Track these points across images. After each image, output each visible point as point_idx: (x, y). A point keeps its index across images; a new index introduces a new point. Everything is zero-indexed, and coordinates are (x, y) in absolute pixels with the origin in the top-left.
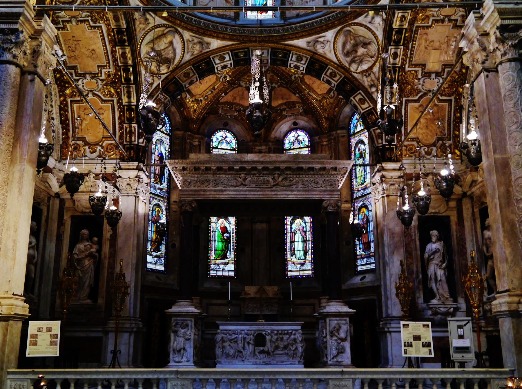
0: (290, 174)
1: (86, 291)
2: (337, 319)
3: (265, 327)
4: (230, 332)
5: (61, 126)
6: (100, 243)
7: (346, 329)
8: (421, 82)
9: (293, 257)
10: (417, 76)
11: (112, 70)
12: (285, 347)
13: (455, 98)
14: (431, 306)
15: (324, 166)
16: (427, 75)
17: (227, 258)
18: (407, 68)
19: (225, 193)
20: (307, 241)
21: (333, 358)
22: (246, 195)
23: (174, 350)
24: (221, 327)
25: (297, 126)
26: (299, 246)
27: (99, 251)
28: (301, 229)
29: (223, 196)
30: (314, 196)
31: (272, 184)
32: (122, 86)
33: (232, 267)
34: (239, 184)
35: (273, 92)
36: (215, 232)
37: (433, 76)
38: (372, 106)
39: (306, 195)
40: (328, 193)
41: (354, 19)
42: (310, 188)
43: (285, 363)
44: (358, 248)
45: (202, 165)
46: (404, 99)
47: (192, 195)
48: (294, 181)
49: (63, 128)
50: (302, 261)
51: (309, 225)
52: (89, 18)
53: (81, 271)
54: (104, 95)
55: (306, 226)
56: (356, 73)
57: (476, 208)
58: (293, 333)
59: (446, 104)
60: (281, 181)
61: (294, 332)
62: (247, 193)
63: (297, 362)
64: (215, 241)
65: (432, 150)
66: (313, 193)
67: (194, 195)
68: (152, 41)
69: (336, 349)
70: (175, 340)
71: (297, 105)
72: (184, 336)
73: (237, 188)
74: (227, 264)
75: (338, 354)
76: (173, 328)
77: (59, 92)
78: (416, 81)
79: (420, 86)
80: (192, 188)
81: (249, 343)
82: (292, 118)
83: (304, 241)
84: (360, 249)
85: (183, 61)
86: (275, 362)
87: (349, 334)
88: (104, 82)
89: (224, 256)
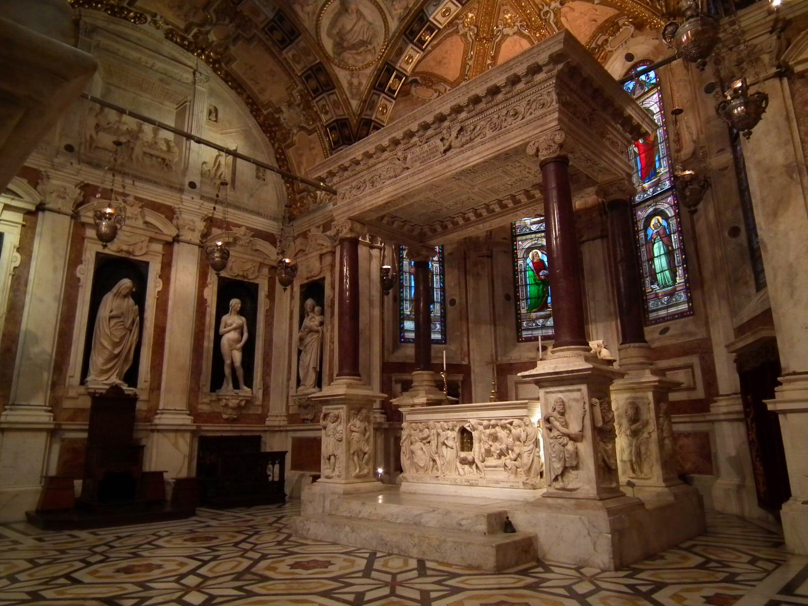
0: (467, 119)
1: (312, 377)
3: (468, 414)
5: (283, 181)
6: (322, 313)
7: (581, 412)
11: (300, 87)
15: (512, 72)
19: (382, 193)
20: (673, 250)
21: (556, 479)
22: (409, 184)
24: (409, 417)
25: (635, 60)
26: (660, 263)
28: (661, 232)
29: (381, 199)
31: (443, 149)
32: (315, 101)
34: (399, 171)
35: (563, 19)
36: (525, 271)
39: (498, 145)
40: (535, 124)
43: (502, 485)
45: (345, 160)
48: (478, 127)
49: (286, 182)
51: (673, 222)
52: (239, 31)
54: (309, 124)
55: (669, 224)
60: (457, 137)
61: (516, 422)
62: (409, 180)
63: (521, 485)
64: (526, 285)
66: (508, 136)
68: (333, 24)
69: (560, 460)
71: (621, 23)
74: (546, 317)
75: (565, 469)
77: (270, 140)
80: (347, 200)
82: (620, 50)
83: (669, 254)
85: (391, 34)
86: (485, 482)
87: (588, 422)
88: (301, 106)
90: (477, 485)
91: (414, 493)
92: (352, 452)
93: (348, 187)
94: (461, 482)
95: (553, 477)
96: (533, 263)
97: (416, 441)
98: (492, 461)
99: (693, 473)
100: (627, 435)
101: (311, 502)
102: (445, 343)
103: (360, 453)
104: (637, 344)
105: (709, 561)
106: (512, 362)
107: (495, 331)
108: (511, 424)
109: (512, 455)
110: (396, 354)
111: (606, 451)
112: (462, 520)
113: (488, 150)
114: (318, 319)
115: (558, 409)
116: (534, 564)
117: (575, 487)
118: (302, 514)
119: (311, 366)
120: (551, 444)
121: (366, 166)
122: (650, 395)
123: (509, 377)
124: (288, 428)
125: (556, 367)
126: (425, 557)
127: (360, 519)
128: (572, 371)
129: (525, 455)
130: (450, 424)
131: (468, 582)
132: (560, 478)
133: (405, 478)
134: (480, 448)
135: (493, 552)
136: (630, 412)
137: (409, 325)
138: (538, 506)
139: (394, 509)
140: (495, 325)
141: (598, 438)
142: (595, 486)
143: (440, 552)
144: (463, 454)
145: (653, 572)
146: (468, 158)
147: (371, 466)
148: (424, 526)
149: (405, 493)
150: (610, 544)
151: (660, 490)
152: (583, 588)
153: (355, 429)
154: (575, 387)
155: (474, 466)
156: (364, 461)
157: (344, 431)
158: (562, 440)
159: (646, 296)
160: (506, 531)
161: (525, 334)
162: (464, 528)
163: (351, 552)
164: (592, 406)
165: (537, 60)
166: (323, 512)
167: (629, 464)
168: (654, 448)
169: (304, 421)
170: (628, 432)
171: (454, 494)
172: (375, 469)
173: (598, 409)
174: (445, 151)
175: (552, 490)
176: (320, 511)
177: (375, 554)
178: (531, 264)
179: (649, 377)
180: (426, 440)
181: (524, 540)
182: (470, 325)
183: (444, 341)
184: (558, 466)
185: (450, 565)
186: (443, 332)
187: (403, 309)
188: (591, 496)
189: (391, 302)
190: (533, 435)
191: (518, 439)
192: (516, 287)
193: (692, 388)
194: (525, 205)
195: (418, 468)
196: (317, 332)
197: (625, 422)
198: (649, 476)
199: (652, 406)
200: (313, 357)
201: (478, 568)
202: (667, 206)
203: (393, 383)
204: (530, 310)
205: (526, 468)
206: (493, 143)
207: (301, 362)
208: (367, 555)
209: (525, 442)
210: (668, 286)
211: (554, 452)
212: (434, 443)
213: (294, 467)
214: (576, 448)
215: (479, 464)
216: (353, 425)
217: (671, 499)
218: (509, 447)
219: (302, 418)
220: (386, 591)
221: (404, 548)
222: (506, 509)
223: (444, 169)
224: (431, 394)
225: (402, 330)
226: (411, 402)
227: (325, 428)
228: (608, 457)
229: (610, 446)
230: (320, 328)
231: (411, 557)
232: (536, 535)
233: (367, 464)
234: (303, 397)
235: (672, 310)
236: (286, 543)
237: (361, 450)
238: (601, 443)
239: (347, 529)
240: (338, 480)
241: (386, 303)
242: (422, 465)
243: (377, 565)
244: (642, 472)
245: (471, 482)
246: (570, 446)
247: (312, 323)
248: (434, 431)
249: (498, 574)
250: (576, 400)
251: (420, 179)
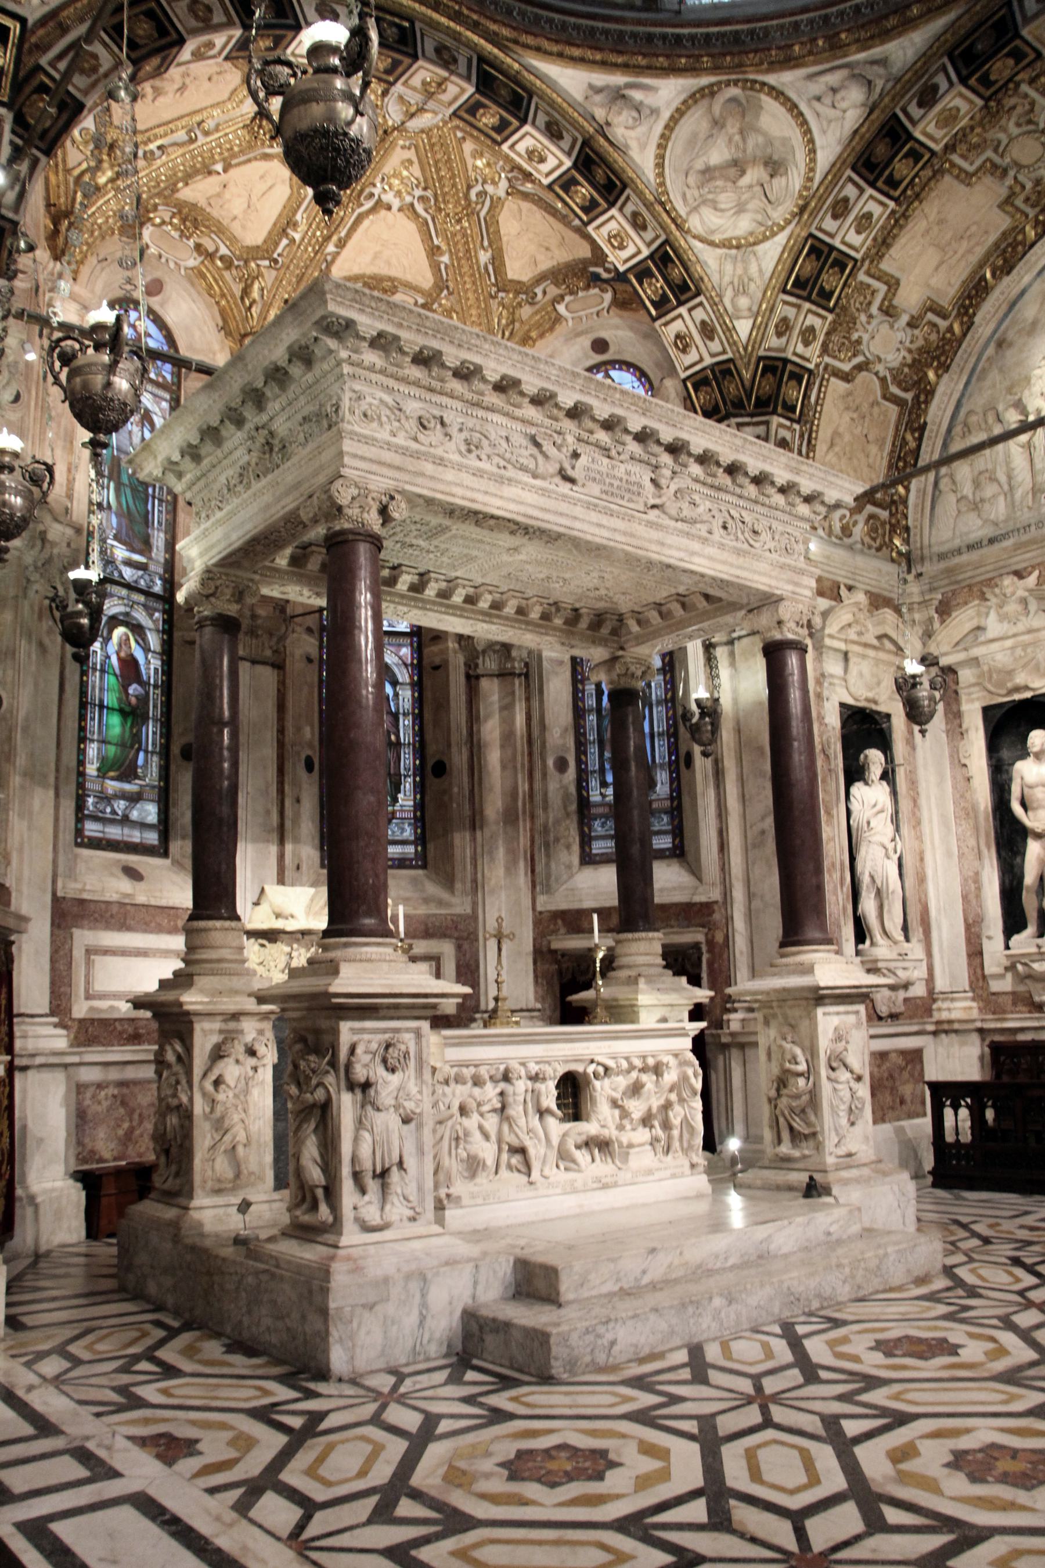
2: (841, 1008)
4: (483, 1071)
8: (874, 322)
10: (870, 303)
13: (916, 397)
14: (880, 965)
15: (797, 479)
16: (889, 311)
17: (137, 777)
18: (862, 277)
20: (398, 744)
22: (575, 518)
23: (357, 1176)
29: (499, 503)
30: (756, 577)
33: (150, 812)
35: (366, 223)
37: (905, 319)
38: (730, 355)
40: (789, 574)
41: (768, 71)
42: (739, 545)
43: (658, 1175)
44: (594, 783)
46: (827, 359)
47: (390, 466)
48: (701, 509)
55: (396, 695)
56: (702, 240)
57: (972, 701)
59: (893, 410)
62: (578, 511)
65: (855, 523)
67: (398, 468)
70: (360, 1124)
72: (397, 1107)
73: (538, 482)
74: (135, 799)
78: (863, 318)
79: (866, 337)
80: (384, 435)
81: (542, 1113)
84: (604, 784)
86: (629, 1175)
90: (615, 1185)
93: (388, 399)
96: (119, 659)
106: (85, 896)
113: (724, 563)
121: (476, 397)
123: (77, 933)
146: (693, 553)
161: (91, 828)
162: (834, 1237)
165: (826, 491)
174: (653, 507)
178: (114, 660)
194: (507, 618)
202: (396, 659)
206: (732, 558)
221: (827, 1292)
223: (650, 541)
239: (717, 1302)
251: (599, 525)
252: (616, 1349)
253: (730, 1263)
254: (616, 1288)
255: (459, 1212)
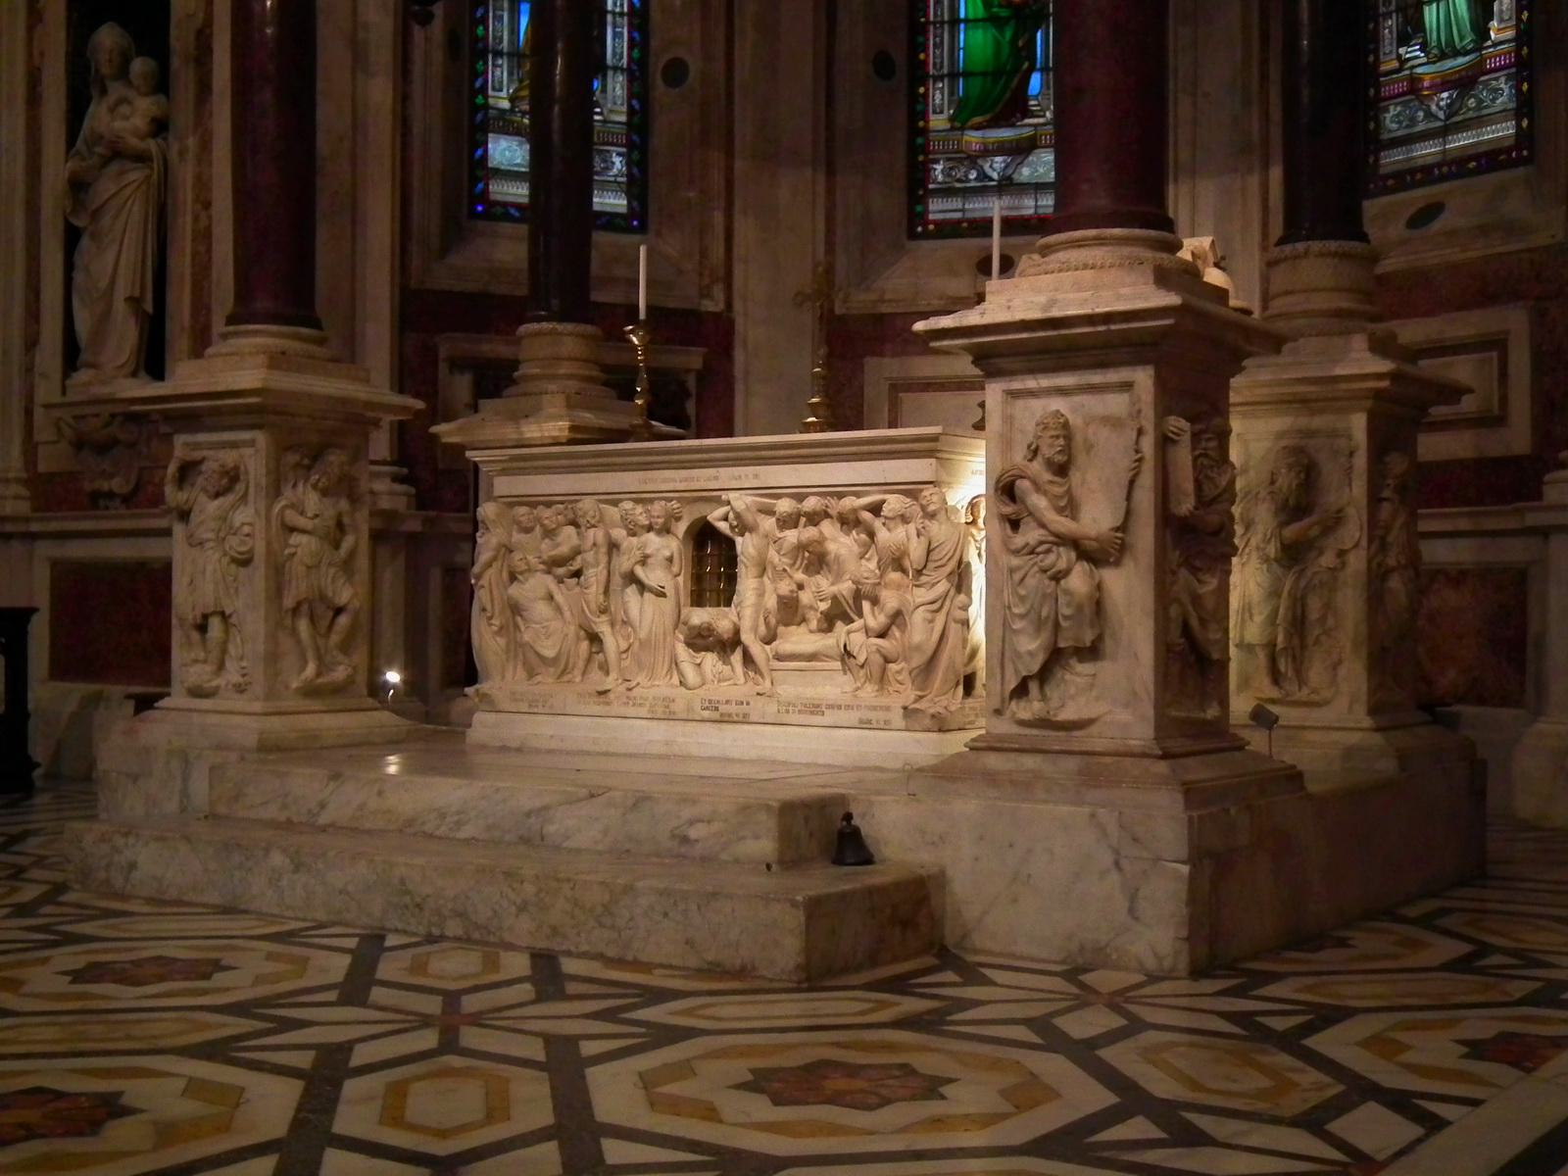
1: (125, 336)
3: (725, 476)
6: (161, 85)
7: (1126, 462)
9: (1413, 52)
12: (836, 615)
17: (1027, 113)
21: (1021, 691)
24: (503, 486)
27: (160, 127)
43: (829, 718)
50: (1461, 60)
53: (94, 236)
58: (886, 510)
61: (894, 503)
63: (897, 718)
64: (955, 22)
74: (1021, 150)
75: (1055, 659)
76: (169, 490)
86: (771, 709)
89: (1015, 107)
90: (745, 720)
91: (519, 750)
92: (289, 602)
94: (690, 709)
95: (1012, 684)
97: (530, 570)
98: (799, 639)
99: (1460, 700)
100: (1266, 560)
101: (135, 778)
102: (643, 229)
103: (322, 610)
104: (1333, 245)
105: (1483, 949)
106: (885, 309)
107: (830, 192)
108: (876, 509)
109: (874, 618)
110: (455, 259)
111: (1196, 599)
112: (692, 823)
114: (145, 107)
115: (1047, 451)
116: (929, 960)
117: (1086, 714)
118: (103, 816)
119: (122, 291)
120: (1012, 571)
122: (1358, 424)
124: (35, 527)
125: (1052, 303)
126: (556, 945)
127: (323, 829)
128: (1108, 318)
129: (919, 617)
130: (658, 508)
131: (708, 1012)
132: (1033, 687)
133: (485, 698)
134: (761, 594)
135: (795, 919)
136: (1286, 481)
137: (507, 151)
138: (953, 779)
139: (447, 792)
140: (831, 172)
141: (1175, 556)
142: (1149, 711)
143: (613, 927)
144: (699, 616)
145: (1310, 981)
147: (360, 656)
148: (557, 848)
149: (483, 747)
150: (1184, 896)
151: (1354, 738)
152: (1082, 1025)
153: (301, 522)
154: (1113, 376)
155: (737, 657)
156: (335, 638)
157: (260, 525)
158: (1052, 557)
159: (1378, 86)
160: (839, 861)
161: (939, 209)
163: (291, 934)
164: (1165, 442)
166: (183, 810)
167: (1262, 657)
168: (1350, 603)
169: (97, 500)
170: (1272, 550)
171: (663, 750)
172: (375, 672)
173: (1183, 457)
175: (1004, 727)
176: (172, 806)
177: (382, 938)
179: (1360, 361)
180: (567, 568)
181: (898, 885)
182: (739, 165)
183: (636, 221)
184: (1031, 647)
185: (637, 965)
186: (636, 185)
187: (483, 90)
188: (1135, 744)
189: (438, 56)
190: (948, 547)
191: (897, 562)
192: (917, 32)
193: (1492, 420)
195: (533, 664)
196: (142, 158)
197: (1264, 516)
198: (1326, 694)
199: (1361, 461)
200: (129, 256)
201: (741, 973)
203: (443, 368)
204: (959, 123)
205: (918, 660)
207: (79, 277)
208: (351, 943)
209: (919, 572)
210: (1457, 53)
211: (1022, 599)
212: (595, 576)
213: (61, 670)
214: (1099, 587)
215: (757, 650)
216: (292, 506)
217: (1387, 766)
218: (864, 589)
219: (88, 487)
220: (429, 1039)
222: (841, 791)
224: (588, 409)
225: (481, 169)
226: (509, 432)
227: (184, 515)
228: (1203, 622)
229: (1213, 583)
230: (152, 145)
231: (510, 947)
232: (942, 873)
233: (346, 647)
234: (95, 409)
235: (1461, 141)
236: (48, 909)
237: (323, 598)
238: (1184, 573)
239: (277, 859)
240: (240, 703)
241: (417, 55)
242: (549, 653)
243: (389, 968)
244: (1302, 682)
245: (723, 708)
246: (1079, 581)
247: (118, 124)
248: (595, 535)
249: (810, 990)
250: (1112, 422)
252: (136, 875)
253: (466, 832)
254: (282, 818)
255: (491, 717)
